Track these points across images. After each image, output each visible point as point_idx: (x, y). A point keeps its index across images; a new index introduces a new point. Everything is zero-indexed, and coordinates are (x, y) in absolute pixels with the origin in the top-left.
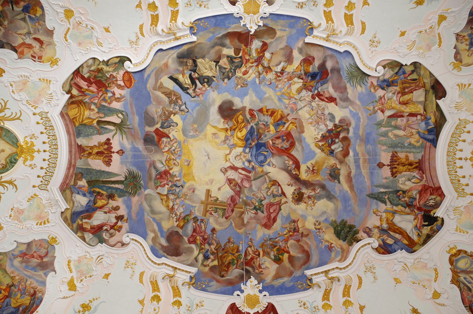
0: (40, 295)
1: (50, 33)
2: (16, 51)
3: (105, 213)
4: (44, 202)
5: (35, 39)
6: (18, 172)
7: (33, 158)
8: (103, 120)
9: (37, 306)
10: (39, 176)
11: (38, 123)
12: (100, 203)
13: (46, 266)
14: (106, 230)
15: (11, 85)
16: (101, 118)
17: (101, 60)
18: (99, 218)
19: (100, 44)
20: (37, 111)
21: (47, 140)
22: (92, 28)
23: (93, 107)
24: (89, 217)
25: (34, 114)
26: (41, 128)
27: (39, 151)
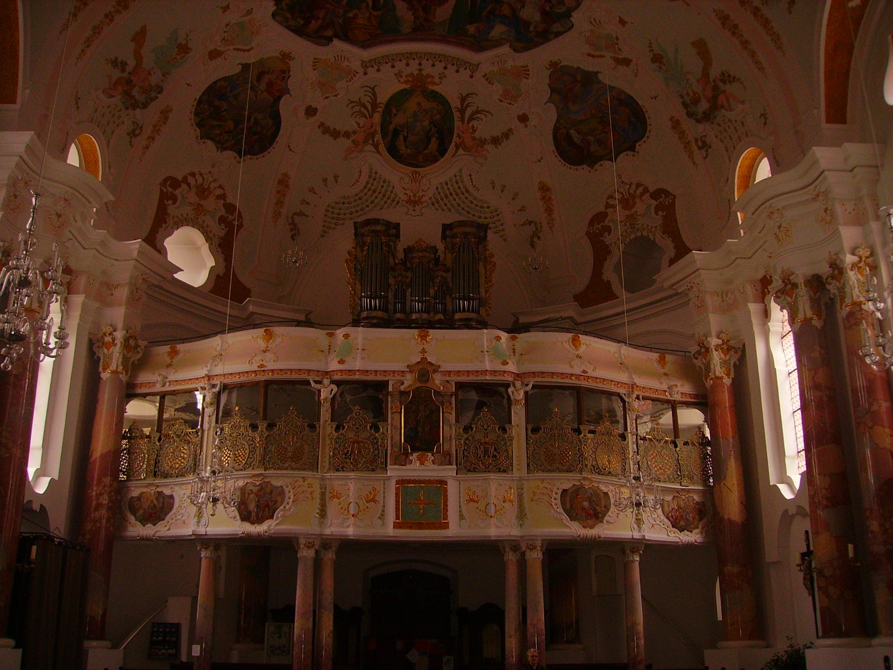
0: (623, 96)
1: (246, 67)
2: (280, 98)
3: (523, 6)
4: (496, 69)
5: (259, 79)
6: (451, 88)
7: (428, 76)
8: (370, 4)
9: (637, 103)
10: (457, 71)
11: (378, 70)
12: (506, 11)
13: (589, 79)
14: (551, 8)
15: (327, 98)
16: (367, 6)
17: (275, 8)
18: (530, 13)
19: (250, 12)
20: (361, 71)
21: (404, 62)
22: (227, 25)
23: (351, 15)
24: (527, 24)
25: (365, 74)
26: (386, 68)
27: (420, 70)
